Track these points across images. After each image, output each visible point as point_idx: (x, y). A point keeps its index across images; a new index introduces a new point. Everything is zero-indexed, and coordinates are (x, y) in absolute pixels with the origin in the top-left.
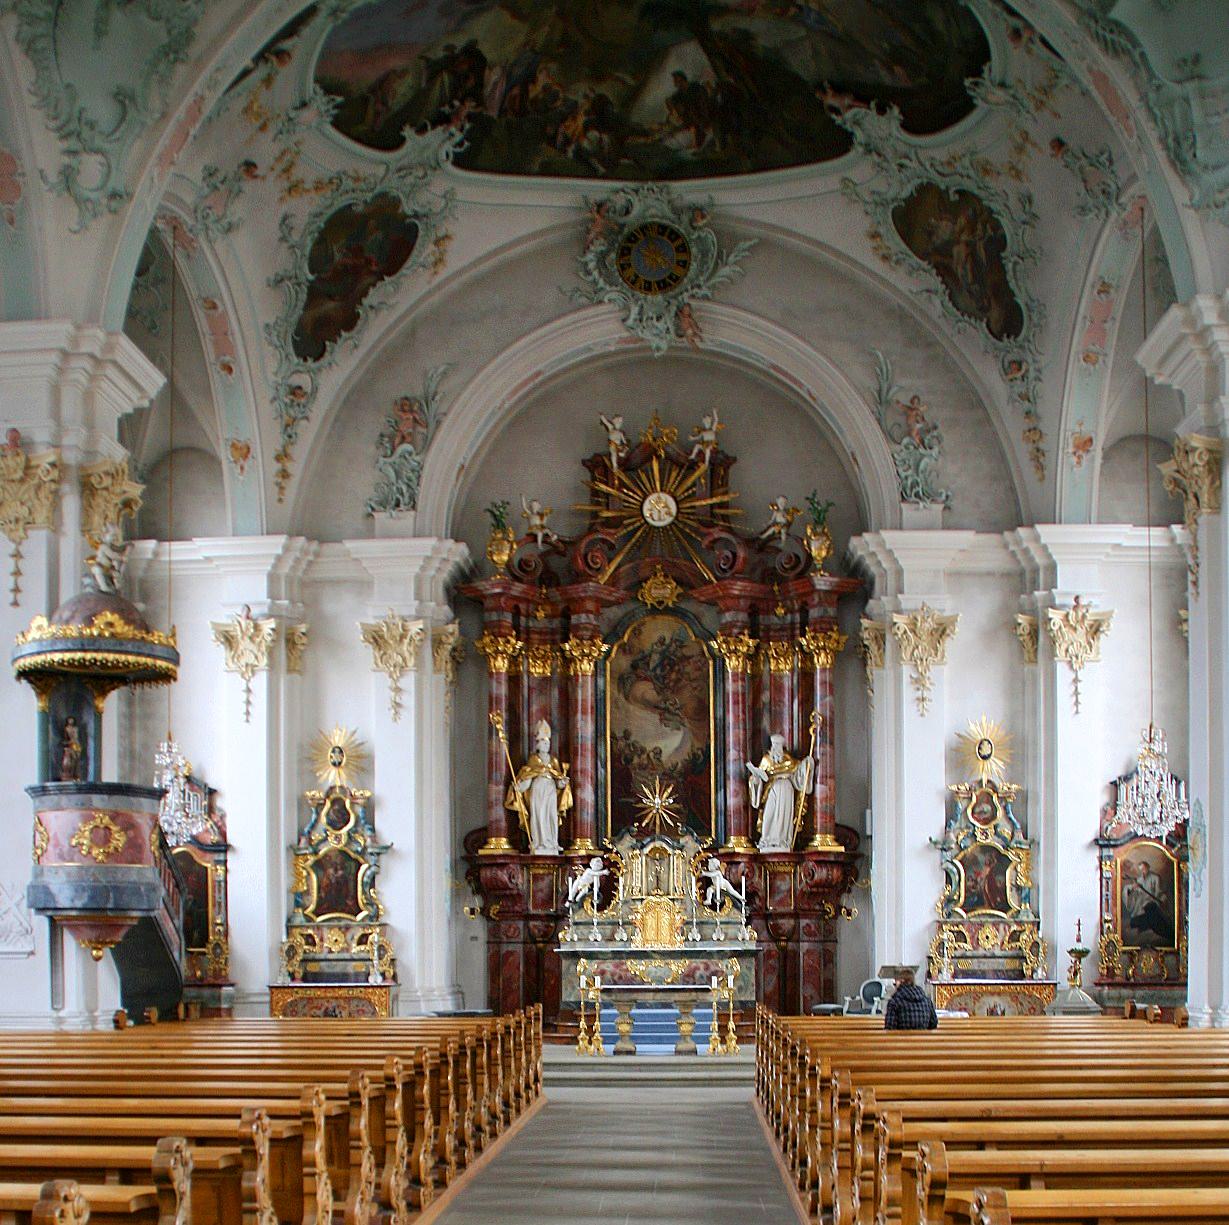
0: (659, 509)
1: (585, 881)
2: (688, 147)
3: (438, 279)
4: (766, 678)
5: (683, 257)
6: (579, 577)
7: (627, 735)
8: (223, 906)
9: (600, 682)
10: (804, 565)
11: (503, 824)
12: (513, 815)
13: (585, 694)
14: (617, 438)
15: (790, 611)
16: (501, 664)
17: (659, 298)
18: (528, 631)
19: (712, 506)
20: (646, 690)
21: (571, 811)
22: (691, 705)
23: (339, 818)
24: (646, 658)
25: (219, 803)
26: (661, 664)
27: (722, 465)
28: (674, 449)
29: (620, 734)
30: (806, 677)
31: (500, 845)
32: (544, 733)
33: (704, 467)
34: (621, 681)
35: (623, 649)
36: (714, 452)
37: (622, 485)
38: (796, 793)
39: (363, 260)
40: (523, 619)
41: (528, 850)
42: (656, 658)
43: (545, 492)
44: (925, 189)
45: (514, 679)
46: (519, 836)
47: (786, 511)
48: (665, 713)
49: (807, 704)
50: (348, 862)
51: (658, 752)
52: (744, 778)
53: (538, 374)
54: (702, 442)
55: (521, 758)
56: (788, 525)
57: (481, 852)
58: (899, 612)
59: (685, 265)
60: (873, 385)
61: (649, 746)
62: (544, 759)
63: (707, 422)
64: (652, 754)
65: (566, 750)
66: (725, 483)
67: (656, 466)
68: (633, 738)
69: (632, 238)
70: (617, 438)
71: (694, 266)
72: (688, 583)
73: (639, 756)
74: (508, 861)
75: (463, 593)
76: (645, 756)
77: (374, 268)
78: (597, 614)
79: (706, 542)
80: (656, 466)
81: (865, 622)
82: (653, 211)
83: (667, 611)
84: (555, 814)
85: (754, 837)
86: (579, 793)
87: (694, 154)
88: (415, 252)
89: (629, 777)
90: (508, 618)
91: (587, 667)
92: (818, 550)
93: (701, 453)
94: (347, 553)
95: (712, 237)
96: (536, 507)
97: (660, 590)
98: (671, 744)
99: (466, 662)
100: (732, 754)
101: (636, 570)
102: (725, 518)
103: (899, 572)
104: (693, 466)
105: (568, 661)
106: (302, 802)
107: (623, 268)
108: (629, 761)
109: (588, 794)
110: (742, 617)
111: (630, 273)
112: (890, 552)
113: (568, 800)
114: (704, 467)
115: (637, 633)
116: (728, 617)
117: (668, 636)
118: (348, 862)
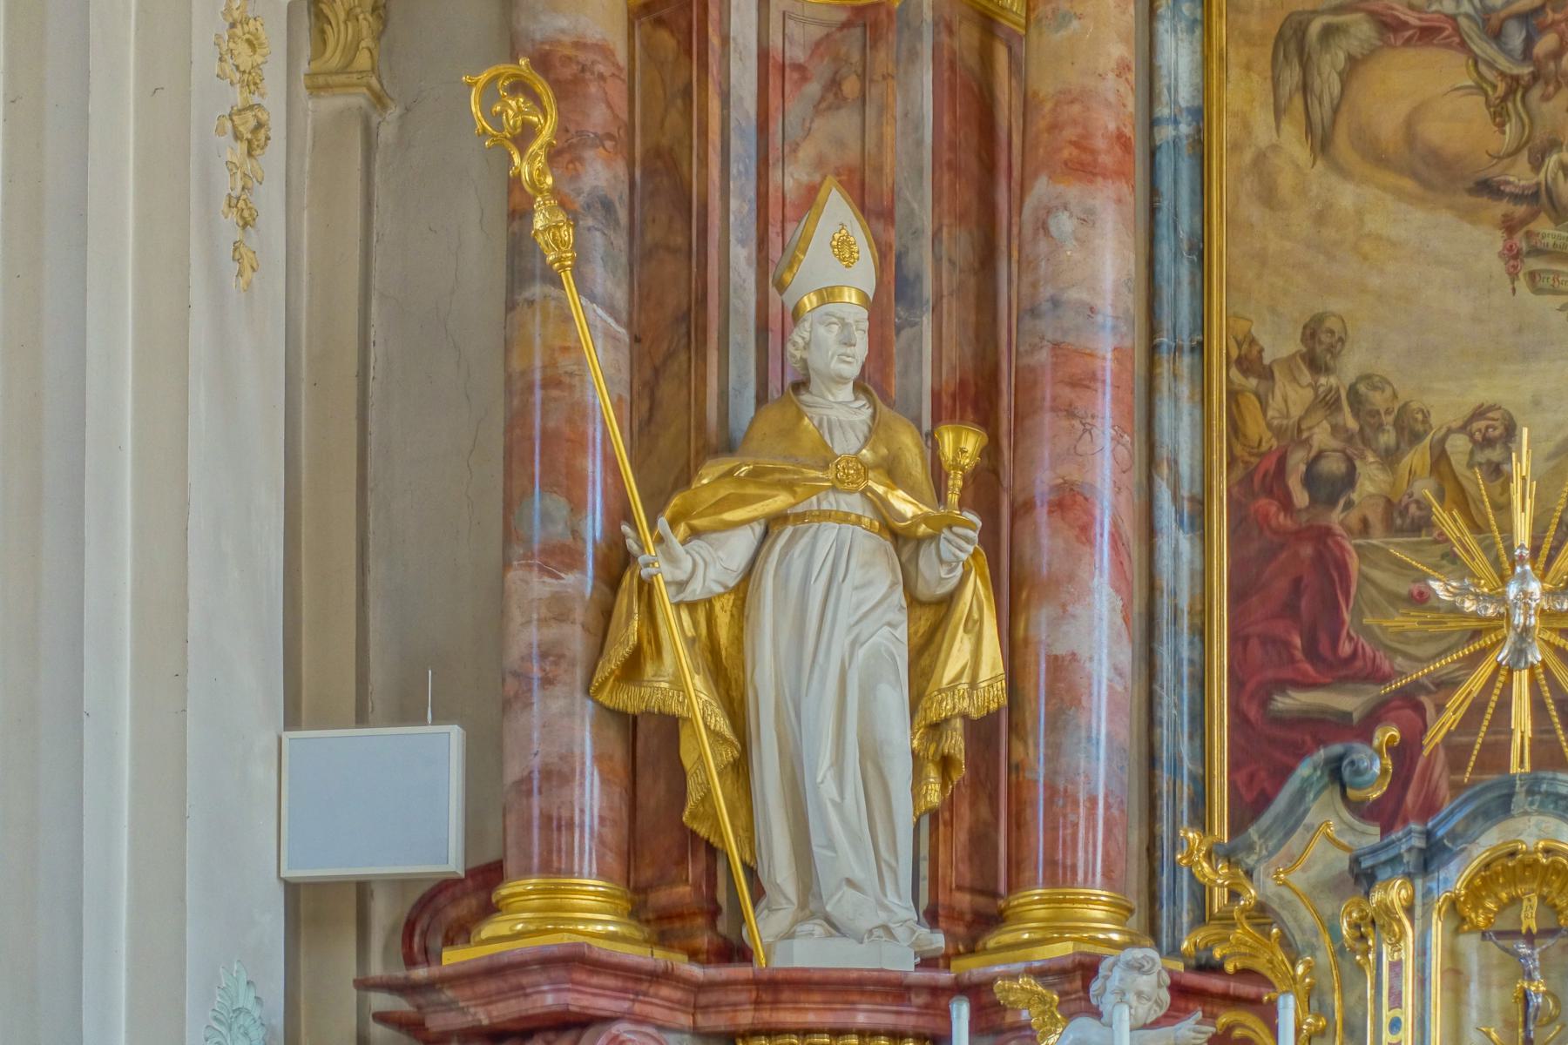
7: (1318, 349)
11: (591, 797)
12: (646, 744)
29: (1279, 345)
32: (835, 270)
41: (734, 951)
46: (681, 873)
57: (454, 957)
61: (1446, 401)
64: (1459, 446)
68: (1351, 366)
73: (1390, 458)
74: (604, 1005)
76: (1417, 458)
84: (899, 738)
86: (1039, 622)
89: (1330, 573)
108: (1331, 488)
113: (974, 661)
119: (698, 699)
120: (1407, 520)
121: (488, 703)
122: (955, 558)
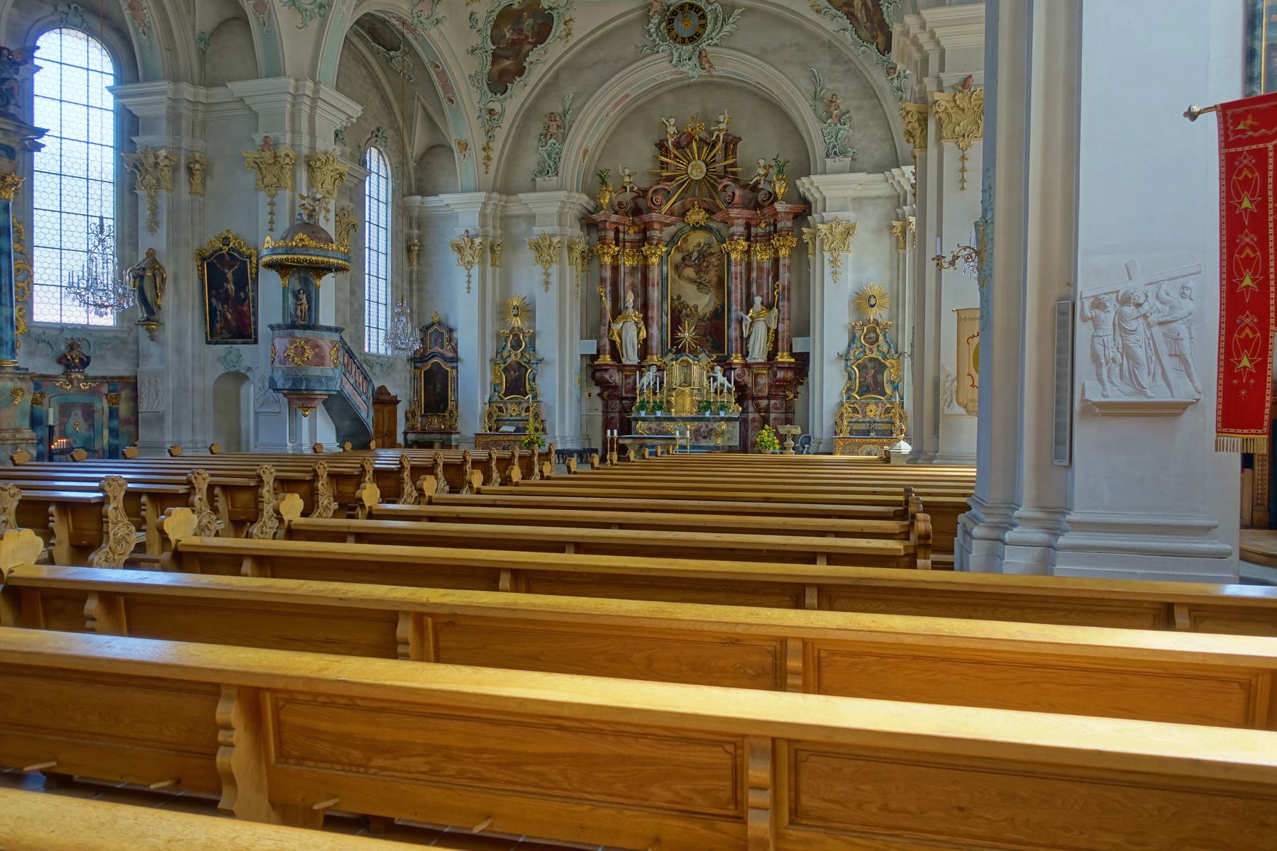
0: (697, 170)
1: (649, 377)
4: (755, 265)
5: (703, 22)
6: (650, 210)
7: (679, 297)
8: (456, 390)
9: (665, 268)
10: (772, 197)
11: (608, 347)
12: (613, 343)
13: (654, 275)
14: (672, 130)
15: (768, 225)
16: (608, 260)
17: (690, 47)
18: (624, 241)
19: (725, 166)
20: (690, 272)
21: (645, 340)
22: (714, 280)
23: (516, 345)
24: (690, 255)
25: (455, 335)
26: (698, 258)
27: (731, 144)
28: (704, 135)
30: (776, 261)
31: (607, 359)
32: (630, 298)
33: (720, 145)
34: (677, 267)
35: (678, 249)
36: (726, 135)
37: (676, 157)
38: (769, 329)
40: (621, 235)
41: (620, 361)
42: (695, 254)
43: (635, 163)
45: (615, 269)
46: (616, 354)
47: (765, 167)
48: (700, 285)
49: (776, 277)
50: (520, 368)
51: (696, 307)
52: (740, 321)
53: (627, 96)
54: (720, 130)
55: (617, 312)
56: (766, 175)
58: (823, 222)
59: (704, 26)
60: (812, 89)
62: (631, 310)
63: (721, 118)
65: (645, 307)
66: (734, 152)
67: (694, 144)
69: (674, 13)
70: (672, 130)
71: (709, 27)
72: (710, 212)
75: (589, 223)
78: (661, 230)
79: (720, 188)
80: (694, 144)
81: (805, 230)
83: (701, 228)
85: (745, 354)
90: (611, 234)
91: (655, 260)
92: (780, 189)
93: (718, 136)
94: (520, 200)
95: (720, 9)
96: (627, 172)
97: (697, 216)
98: (703, 302)
99: (590, 256)
100: (734, 307)
101: (683, 205)
102: (734, 173)
103: (825, 199)
104: (714, 146)
105: (646, 258)
106: (498, 336)
107: (669, 31)
108: (680, 312)
109: (655, 331)
110: (741, 229)
111: (672, 33)
112: (818, 188)
113: (643, 334)
114: (720, 145)
115: (685, 240)
116: (733, 230)
117: (702, 242)
118: (520, 368)
119: (617, 339)
120: (687, 316)
121: (599, 338)
122: (642, 325)
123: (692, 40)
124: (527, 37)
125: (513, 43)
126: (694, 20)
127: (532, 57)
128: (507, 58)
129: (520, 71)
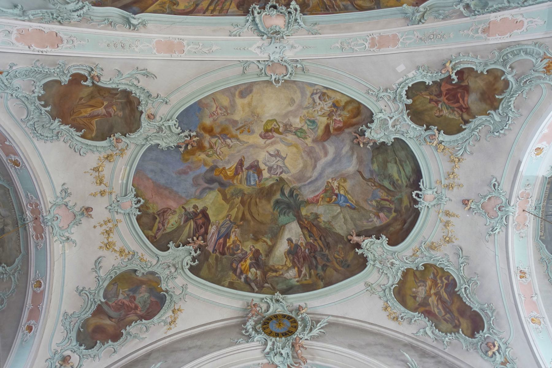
2: (295, 278)
3: (170, 333)
5: (295, 324)
39: (133, 305)
44: (405, 274)
77: (138, 312)
82: (279, 310)
87: (298, 281)
88: (162, 312)
111: (267, 331)
123: (285, 335)
124: (136, 308)
125: (120, 307)
126: (287, 324)
127: (133, 329)
128: (110, 318)
129: (116, 337)
